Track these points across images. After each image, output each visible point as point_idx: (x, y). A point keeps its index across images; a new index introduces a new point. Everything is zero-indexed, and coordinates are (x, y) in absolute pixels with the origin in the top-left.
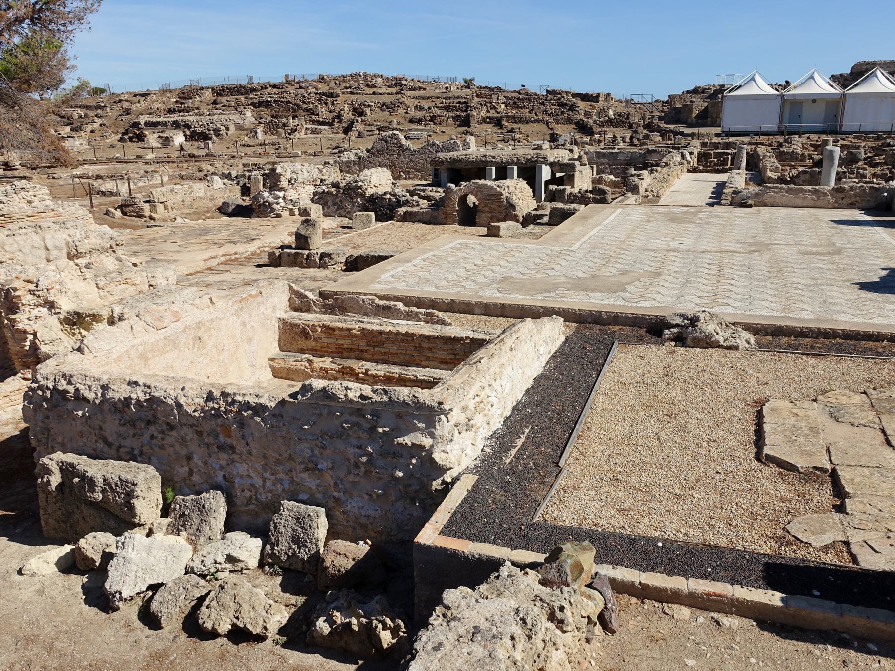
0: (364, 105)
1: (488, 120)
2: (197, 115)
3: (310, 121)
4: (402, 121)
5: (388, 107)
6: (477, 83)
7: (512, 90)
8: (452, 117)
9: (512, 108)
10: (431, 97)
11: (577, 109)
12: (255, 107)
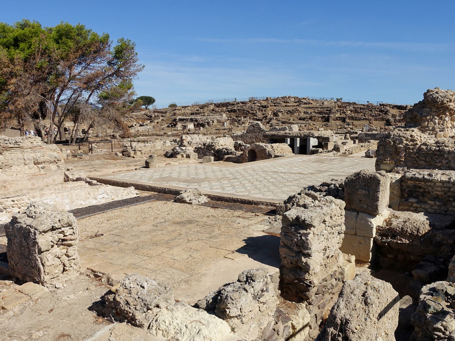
0: (279, 111)
1: (339, 119)
2: (202, 116)
3: (252, 119)
4: (295, 119)
5: (291, 112)
6: (343, 101)
7: (361, 104)
8: (321, 117)
9: (354, 113)
10: (314, 107)
11: (388, 113)
12: (229, 112)
